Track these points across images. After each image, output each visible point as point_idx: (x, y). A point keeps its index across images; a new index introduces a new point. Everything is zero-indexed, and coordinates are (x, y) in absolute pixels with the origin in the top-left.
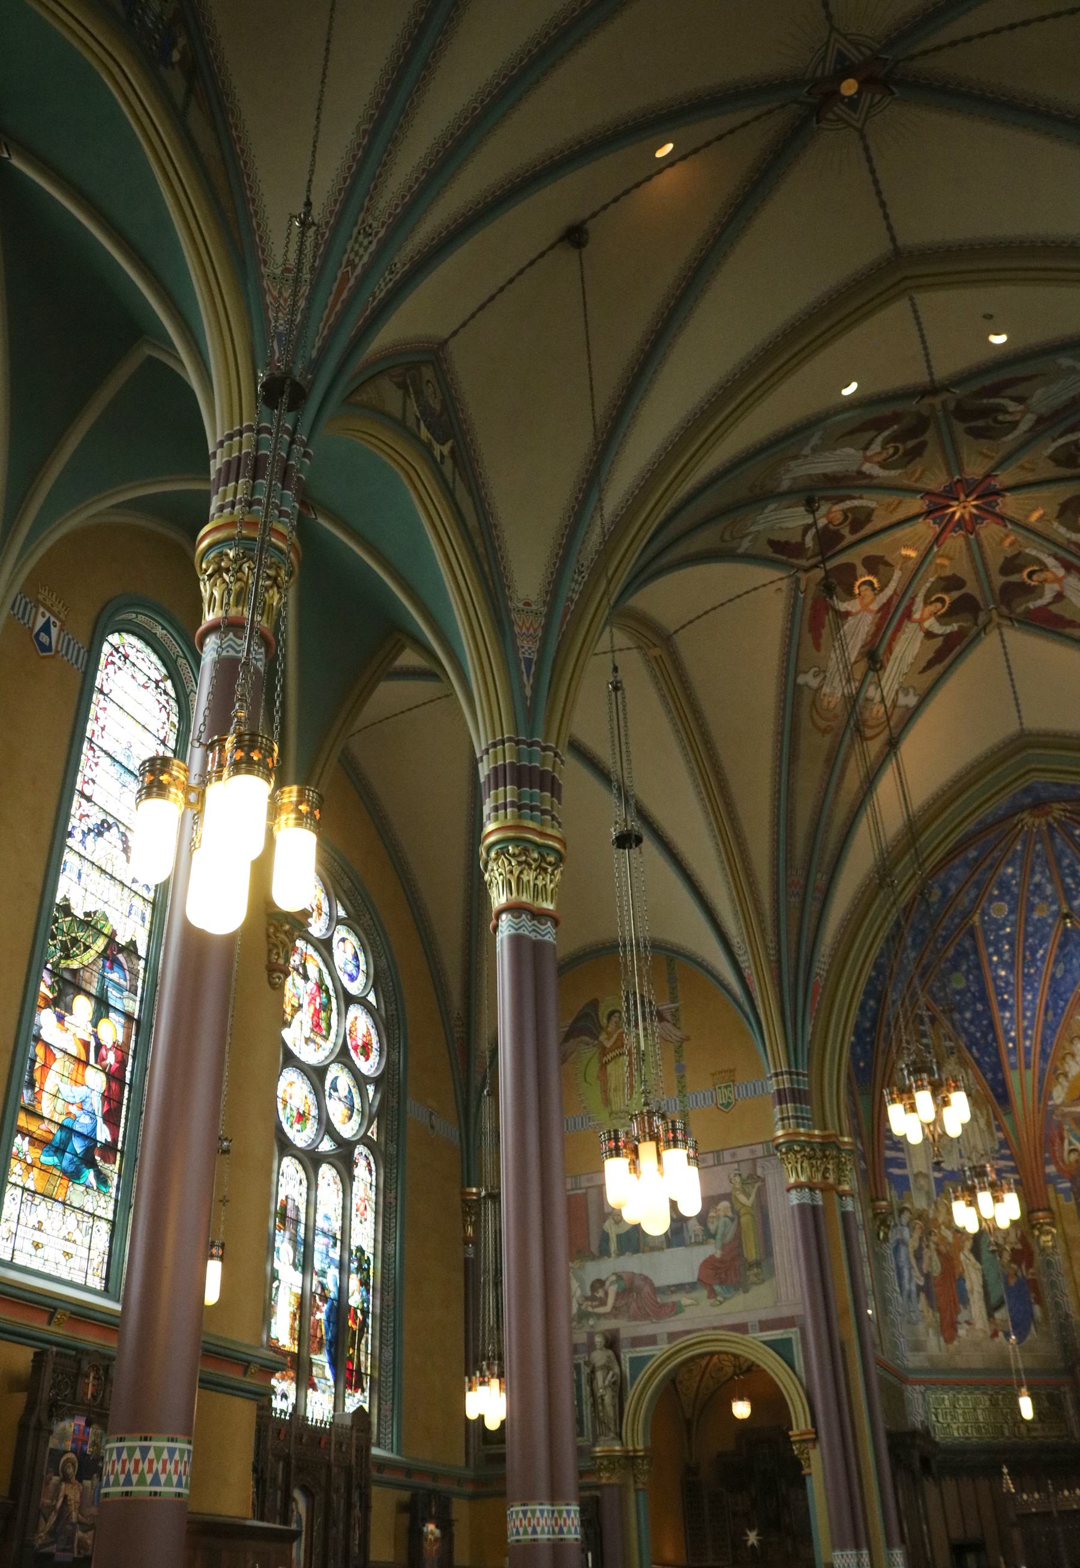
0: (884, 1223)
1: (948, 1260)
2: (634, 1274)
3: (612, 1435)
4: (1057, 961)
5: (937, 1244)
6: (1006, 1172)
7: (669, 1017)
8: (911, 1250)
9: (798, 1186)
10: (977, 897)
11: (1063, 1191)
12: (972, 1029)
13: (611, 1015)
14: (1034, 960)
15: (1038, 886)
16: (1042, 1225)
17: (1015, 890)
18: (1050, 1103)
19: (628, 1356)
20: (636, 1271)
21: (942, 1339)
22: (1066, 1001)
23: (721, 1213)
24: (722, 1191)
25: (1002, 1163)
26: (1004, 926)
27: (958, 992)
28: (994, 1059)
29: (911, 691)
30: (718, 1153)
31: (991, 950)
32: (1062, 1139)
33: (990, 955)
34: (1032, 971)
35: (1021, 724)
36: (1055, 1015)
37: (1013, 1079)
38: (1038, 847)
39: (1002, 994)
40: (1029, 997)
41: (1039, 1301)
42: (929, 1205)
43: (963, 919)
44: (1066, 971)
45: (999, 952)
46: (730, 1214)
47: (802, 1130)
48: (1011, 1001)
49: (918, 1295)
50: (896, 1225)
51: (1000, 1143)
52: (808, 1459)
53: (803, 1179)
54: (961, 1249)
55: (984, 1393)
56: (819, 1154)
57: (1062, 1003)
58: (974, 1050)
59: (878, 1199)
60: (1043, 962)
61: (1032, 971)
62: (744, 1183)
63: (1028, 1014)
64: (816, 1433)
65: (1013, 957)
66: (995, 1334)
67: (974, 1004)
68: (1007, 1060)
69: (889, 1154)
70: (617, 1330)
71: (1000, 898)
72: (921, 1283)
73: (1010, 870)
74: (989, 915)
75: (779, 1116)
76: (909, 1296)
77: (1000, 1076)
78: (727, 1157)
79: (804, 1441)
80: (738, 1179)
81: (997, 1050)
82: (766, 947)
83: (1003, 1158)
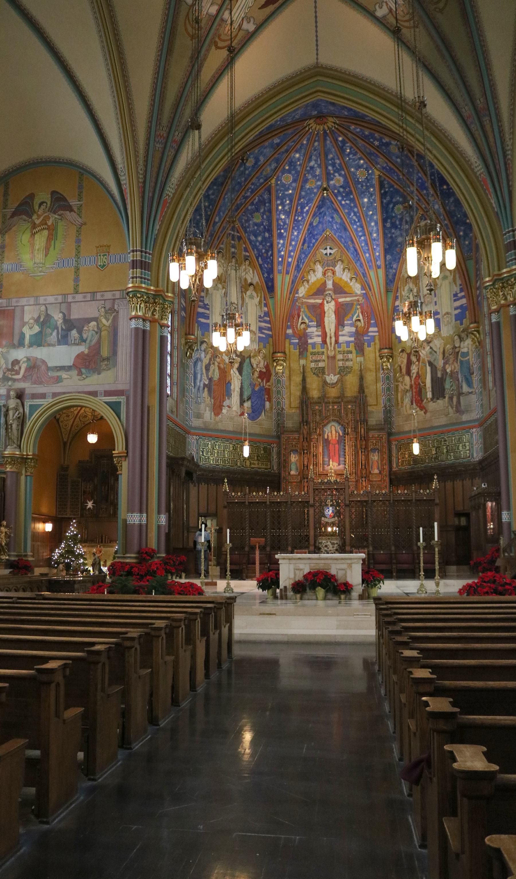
0: (190, 347)
1: (224, 373)
2: (37, 358)
3: (15, 446)
4: (314, 215)
5: (219, 363)
6: (265, 329)
7: (76, 210)
8: (204, 365)
9: (136, 317)
11: (294, 344)
12: (261, 247)
13: (41, 204)
14: (302, 212)
15: (312, 168)
16: (279, 360)
17: (299, 168)
18: (297, 295)
19: (29, 403)
20: (39, 357)
22: (317, 240)
23: (91, 329)
24: (93, 316)
25: (263, 325)
27: (256, 224)
28: (270, 266)
29: (252, 20)
30: (94, 293)
31: (279, 202)
33: (278, 205)
34: (300, 218)
35: (317, 59)
36: (308, 247)
37: (278, 279)
38: (316, 144)
39: (280, 229)
40: (296, 233)
41: (269, 400)
43: (266, 180)
44: (319, 222)
45: (283, 204)
46: (96, 329)
47: (143, 285)
48: (285, 234)
49: (204, 389)
50: (197, 350)
51: (265, 313)
52: (121, 466)
53: (140, 314)
54: (232, 367)
55: (230, 443)
56: (152, 300)
57: (314, 241)
58: (260, 259)
59: (189, 334)
60: (307, 215)
61: (300, 218)
62: (106, 312)
64: (127, 453)
65: (290, 208)
66: (242, 414)
67: (264, 232)
68: (277, 268)
69: (200, 310)
70: (24, 389)
71: (289, 171)
72: (207, 383)
73: (297, 155)
74: (281, 180)
75: (131, 276)
76: (199, 389)
77: (271, 276)
78: (98, 296)
79: (120, 457)
80: (103, 309)
81: (272, 261)
82: (138, 172)
83: (265, 322)
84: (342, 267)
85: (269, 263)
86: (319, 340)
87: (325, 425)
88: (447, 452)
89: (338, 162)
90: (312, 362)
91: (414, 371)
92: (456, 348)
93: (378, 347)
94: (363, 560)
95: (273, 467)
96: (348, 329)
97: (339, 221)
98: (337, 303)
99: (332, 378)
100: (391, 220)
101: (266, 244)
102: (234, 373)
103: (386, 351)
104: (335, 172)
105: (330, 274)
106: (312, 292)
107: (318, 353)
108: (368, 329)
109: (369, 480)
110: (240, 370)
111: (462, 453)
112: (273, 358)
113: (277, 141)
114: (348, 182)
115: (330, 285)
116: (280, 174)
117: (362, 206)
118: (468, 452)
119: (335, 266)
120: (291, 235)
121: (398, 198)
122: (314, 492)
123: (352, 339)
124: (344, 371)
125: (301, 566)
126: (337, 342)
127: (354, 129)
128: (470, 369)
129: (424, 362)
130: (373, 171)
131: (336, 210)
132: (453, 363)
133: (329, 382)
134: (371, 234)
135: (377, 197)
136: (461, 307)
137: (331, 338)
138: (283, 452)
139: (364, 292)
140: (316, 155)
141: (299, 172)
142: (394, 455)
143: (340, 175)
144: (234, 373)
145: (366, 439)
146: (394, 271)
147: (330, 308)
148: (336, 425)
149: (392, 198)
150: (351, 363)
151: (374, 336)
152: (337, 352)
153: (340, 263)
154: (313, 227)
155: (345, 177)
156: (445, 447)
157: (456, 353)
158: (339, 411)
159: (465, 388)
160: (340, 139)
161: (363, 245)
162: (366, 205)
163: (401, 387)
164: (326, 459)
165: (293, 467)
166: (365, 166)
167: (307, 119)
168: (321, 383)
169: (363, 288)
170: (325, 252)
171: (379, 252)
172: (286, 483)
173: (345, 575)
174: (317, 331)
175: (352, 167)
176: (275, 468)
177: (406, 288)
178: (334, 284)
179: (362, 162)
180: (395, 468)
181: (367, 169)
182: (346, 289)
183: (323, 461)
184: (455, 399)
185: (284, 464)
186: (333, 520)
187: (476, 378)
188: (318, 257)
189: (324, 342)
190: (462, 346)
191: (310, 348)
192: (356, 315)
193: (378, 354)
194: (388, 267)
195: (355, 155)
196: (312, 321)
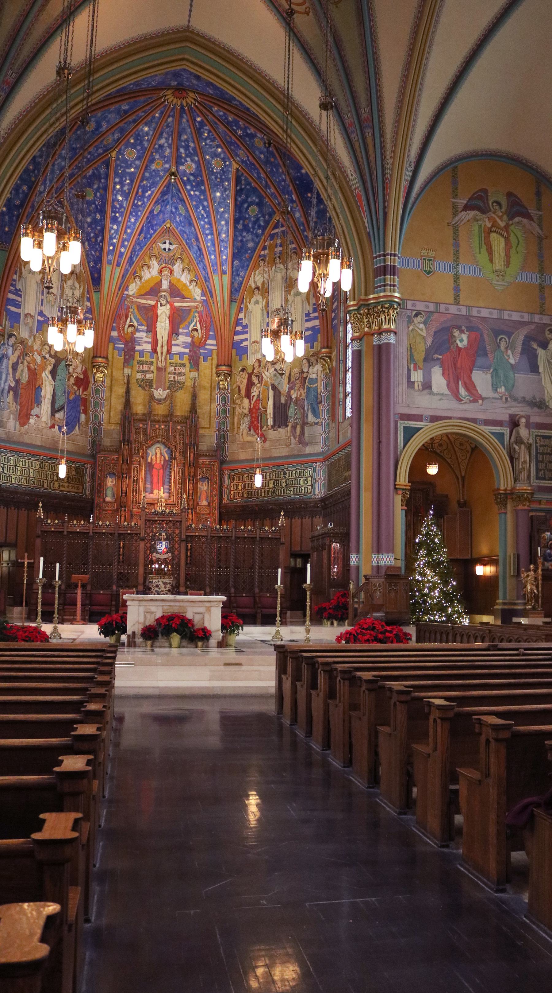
1: (34, 374)
5: (29, 363)
8: (11, 363)
10: (118, 139)
11: (118, 349)
14: (143, 196)
15: (161, 146)
16: (100, 366)
17: (146, 144)
18: (126, 292)
21: (18, 422)
22: (155, 231)
26: (130, 167)
28: (98, 254)
31: (117, 180)
32: (127, 317)
33: (116, 183)
34: (140, 203)
35: (189, 21)
36: (145, 238)
37: (107, 271)
38: (170, 119)
39: (115, 213)
40: (133, 220)
41: (85, 412)
42: (30, 337)
43: (105, 151)
44: (160, 211)
45: (122, 183)
48: (120, 219)
49: (9, 392)
54: (44, 369)
55: (37, 460)
57: (152, 232)
60: (148, 200)
61: (140, 203)
63: (129, 231)
65: (130, 190)
66: (53, 426)
67: (95, 213)
68: (106, 257)
71: (134, 146)
72: (13, 385)
73: (146, 129)
74: (123, 155)
81: (102, 248)
84: (181, 267)
85: (97, 249)
86: (149, 347)
87: (149, 447)
88: (286, 486)
89: (192, 145)
90: (138, 372)
91: (253, 394)
92: (304, 372)
93: (215, 362)
94: (223, 603)
95: (85, 490)
96: (183, 339)
97: (183, 212)
98: (172, 306)
99: (160, 393)
100: (244, 222)
101: (96, 227)
102: (46, 376)
103: (224, 368)
104: (187, 156)
105: (166, 272)
106: (144, 292)
107: (146, 363)
108: (205, 341)
109: (196, 513)
110: (53, 373)
111: (303, 488)
112: (93, 363)
113: (125, 107)
114: (201, 171)
115: (165, 285)
116: (123, 147)
117: (213, 200)
118: (309, 487)
119: (173, 264)
120: (128, 221)
121: (254, 198)
122: (146, 524)
123: (187, 350)
124: (174, 386)
125: (153, 609)
126: (169, 352)
127: (216, 111)
128: (317, 398)
129: (266, 385)
131: (182, 200)
132: (299, 389)
133: (156, 397)
134: (219, 234)
135: (231, 193)
136: (313, 328)
137: (162, 346)
138: (98, 474)
139: (204, 298)
140: (168, 133)
141: (146, 148)
142: (226, 485)
143: (192, 161)
144: (46, 376)
145: (195, 465)
146: (241, 279)
147: (163, 312)
148: (162, 447)
149: (247, 197)
150: (184, 377)
151: (212, 350)
152: (168, 363)
154: (153, 215)
156: (284, 481)
157: (303, 378)
158: (167, 431)
159: (311, 418)
160: (199, 119)
161: (209, 244)
162: (218, 200)
163: (238, 410)
164: (148, 486)
165: (109, 493)
167: (165, 89)
168: (147, 398)
169: (203, 294)
170: (163, 246)
171: (226, 255)
172: (99, 510)
173: (203, 619)
174: (146, 337)
175: (208, 154)
176: (88, 492)
177: (253, 300)
178: (171, 285)
180: (225, 502)
181: (224, 160)
182: (184, 293)
183: (145, 488)
184: (298, 429)
186: (165, 556)
187: (323, 408)
188: (155, 251)
189: (154, 350)
190: (310, 371)
191: (137, 355)
192: (194, 323)
193: (214, 371)
194: (235, 274)
196: (142, 325)
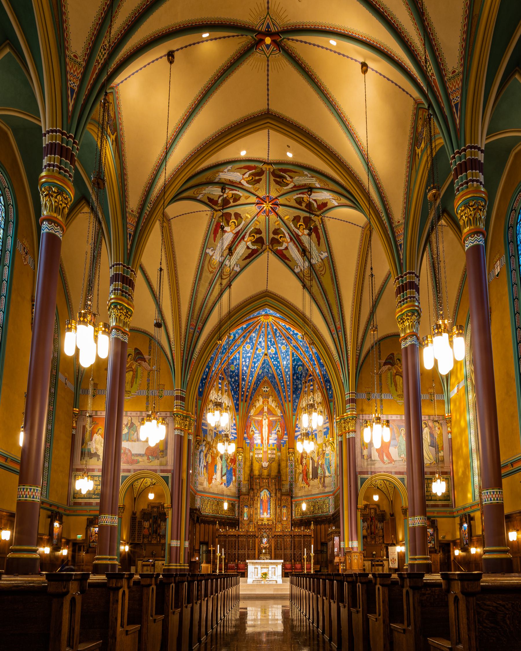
115: (266, 409)
130: (289, 348)
138: (241, 506)
147: (265, 423)
153: (271, 396)
155: (275, 348)
166: (285, 344)
178: (268, 409)
179: (284, 341)
181: (286, 345)
185: (241, 513)
191: (255, 445)
195: (281, 337)
